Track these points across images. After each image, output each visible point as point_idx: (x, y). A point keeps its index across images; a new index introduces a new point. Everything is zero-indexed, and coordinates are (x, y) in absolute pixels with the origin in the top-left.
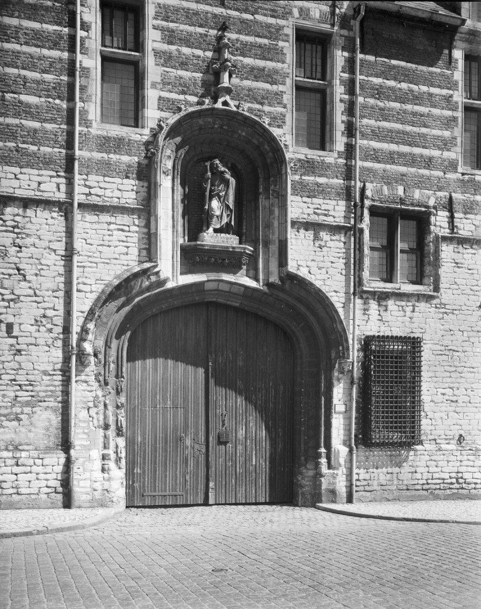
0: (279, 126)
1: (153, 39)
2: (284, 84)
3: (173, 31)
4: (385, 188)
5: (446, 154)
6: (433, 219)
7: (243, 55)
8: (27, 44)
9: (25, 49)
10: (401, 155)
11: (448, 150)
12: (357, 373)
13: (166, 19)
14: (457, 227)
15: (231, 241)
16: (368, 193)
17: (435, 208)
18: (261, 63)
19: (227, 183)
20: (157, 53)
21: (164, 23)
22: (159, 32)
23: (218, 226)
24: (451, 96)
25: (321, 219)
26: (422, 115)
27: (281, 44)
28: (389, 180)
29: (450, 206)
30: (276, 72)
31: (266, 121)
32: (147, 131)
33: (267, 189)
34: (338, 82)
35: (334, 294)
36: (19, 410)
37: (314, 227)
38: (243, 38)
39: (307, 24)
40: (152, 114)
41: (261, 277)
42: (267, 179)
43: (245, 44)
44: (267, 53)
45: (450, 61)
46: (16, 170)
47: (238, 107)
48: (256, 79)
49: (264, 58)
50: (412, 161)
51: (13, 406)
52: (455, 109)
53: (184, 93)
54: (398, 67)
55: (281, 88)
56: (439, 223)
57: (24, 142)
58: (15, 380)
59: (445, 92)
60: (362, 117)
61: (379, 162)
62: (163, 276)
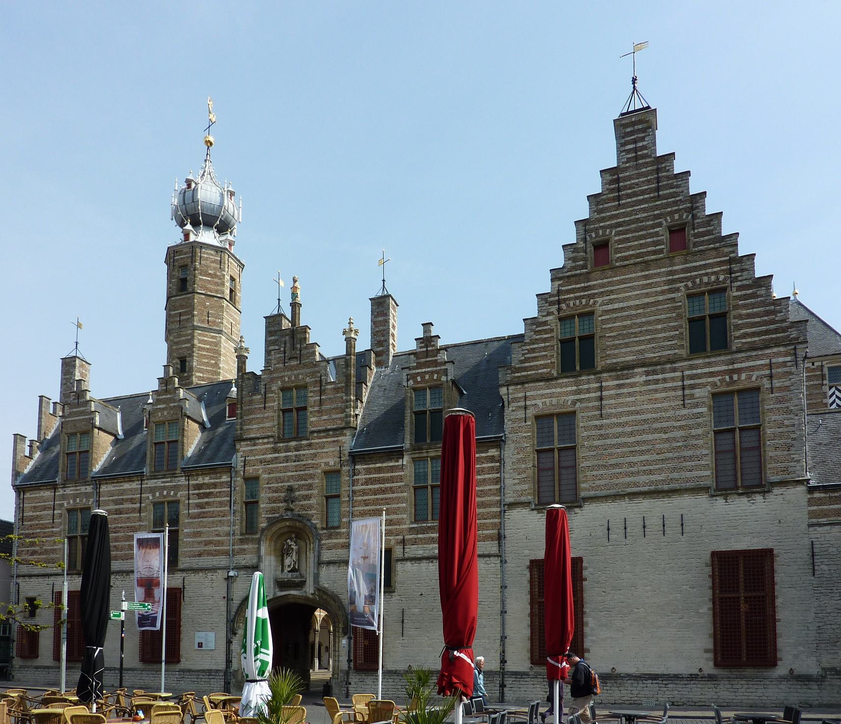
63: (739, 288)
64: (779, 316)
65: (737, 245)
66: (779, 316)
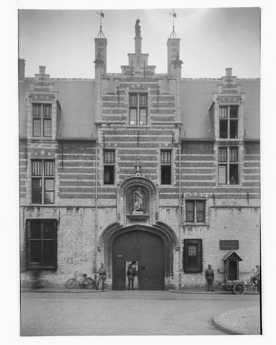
0: (155, 179)
1: (118, 160)
2: (157, 166)
3: (123, 156)
4: (190, 194)
5: (211, 181)
6: (207, 202)
7: (144, 160)
10: (195, 183)
11: (212, 180)
12: (182, 250)
13: (122, 154)
14: (216, 203)
15: (141, 213)
16: (185, 196)
17: (208, 198)
18: (149, 162)
19: (140, 197)
20: (119, 163)
21: (120, 155)
22: (119, 158)
23: (137, 209)
24: (213, 163)
25: (169, 205)
26: (202, 170)
27: (156, 155)
28: (192, 191)
29: (214, 197)
30: (154, 163)
31: (150, 179)
32: (116, 185)
33: (152, 198)
34: (174, 164)
35: (174, 227)
37: (168, 208)
38: (144, 155)
39: (164, 148)
40: (117, 180)
41: (151, 223)
42: (152, 194)
43: (144, 157)
44: (150, 158)
45: (213, 152)
46: (81, 199)
47: (141, 175)
48: (148, 166)
49: (151, 160)
50: (200, 184)
51: (81, 261)
52: (215, 166)
53: (127, 173)
54: (194, 156)
55: (156, 168)
56: (210, 203)
57: (83, 192)
58: (81, 254)
59: (211, 162)
60: (183, 173)
61: (188, 186)
62: (121, 225)
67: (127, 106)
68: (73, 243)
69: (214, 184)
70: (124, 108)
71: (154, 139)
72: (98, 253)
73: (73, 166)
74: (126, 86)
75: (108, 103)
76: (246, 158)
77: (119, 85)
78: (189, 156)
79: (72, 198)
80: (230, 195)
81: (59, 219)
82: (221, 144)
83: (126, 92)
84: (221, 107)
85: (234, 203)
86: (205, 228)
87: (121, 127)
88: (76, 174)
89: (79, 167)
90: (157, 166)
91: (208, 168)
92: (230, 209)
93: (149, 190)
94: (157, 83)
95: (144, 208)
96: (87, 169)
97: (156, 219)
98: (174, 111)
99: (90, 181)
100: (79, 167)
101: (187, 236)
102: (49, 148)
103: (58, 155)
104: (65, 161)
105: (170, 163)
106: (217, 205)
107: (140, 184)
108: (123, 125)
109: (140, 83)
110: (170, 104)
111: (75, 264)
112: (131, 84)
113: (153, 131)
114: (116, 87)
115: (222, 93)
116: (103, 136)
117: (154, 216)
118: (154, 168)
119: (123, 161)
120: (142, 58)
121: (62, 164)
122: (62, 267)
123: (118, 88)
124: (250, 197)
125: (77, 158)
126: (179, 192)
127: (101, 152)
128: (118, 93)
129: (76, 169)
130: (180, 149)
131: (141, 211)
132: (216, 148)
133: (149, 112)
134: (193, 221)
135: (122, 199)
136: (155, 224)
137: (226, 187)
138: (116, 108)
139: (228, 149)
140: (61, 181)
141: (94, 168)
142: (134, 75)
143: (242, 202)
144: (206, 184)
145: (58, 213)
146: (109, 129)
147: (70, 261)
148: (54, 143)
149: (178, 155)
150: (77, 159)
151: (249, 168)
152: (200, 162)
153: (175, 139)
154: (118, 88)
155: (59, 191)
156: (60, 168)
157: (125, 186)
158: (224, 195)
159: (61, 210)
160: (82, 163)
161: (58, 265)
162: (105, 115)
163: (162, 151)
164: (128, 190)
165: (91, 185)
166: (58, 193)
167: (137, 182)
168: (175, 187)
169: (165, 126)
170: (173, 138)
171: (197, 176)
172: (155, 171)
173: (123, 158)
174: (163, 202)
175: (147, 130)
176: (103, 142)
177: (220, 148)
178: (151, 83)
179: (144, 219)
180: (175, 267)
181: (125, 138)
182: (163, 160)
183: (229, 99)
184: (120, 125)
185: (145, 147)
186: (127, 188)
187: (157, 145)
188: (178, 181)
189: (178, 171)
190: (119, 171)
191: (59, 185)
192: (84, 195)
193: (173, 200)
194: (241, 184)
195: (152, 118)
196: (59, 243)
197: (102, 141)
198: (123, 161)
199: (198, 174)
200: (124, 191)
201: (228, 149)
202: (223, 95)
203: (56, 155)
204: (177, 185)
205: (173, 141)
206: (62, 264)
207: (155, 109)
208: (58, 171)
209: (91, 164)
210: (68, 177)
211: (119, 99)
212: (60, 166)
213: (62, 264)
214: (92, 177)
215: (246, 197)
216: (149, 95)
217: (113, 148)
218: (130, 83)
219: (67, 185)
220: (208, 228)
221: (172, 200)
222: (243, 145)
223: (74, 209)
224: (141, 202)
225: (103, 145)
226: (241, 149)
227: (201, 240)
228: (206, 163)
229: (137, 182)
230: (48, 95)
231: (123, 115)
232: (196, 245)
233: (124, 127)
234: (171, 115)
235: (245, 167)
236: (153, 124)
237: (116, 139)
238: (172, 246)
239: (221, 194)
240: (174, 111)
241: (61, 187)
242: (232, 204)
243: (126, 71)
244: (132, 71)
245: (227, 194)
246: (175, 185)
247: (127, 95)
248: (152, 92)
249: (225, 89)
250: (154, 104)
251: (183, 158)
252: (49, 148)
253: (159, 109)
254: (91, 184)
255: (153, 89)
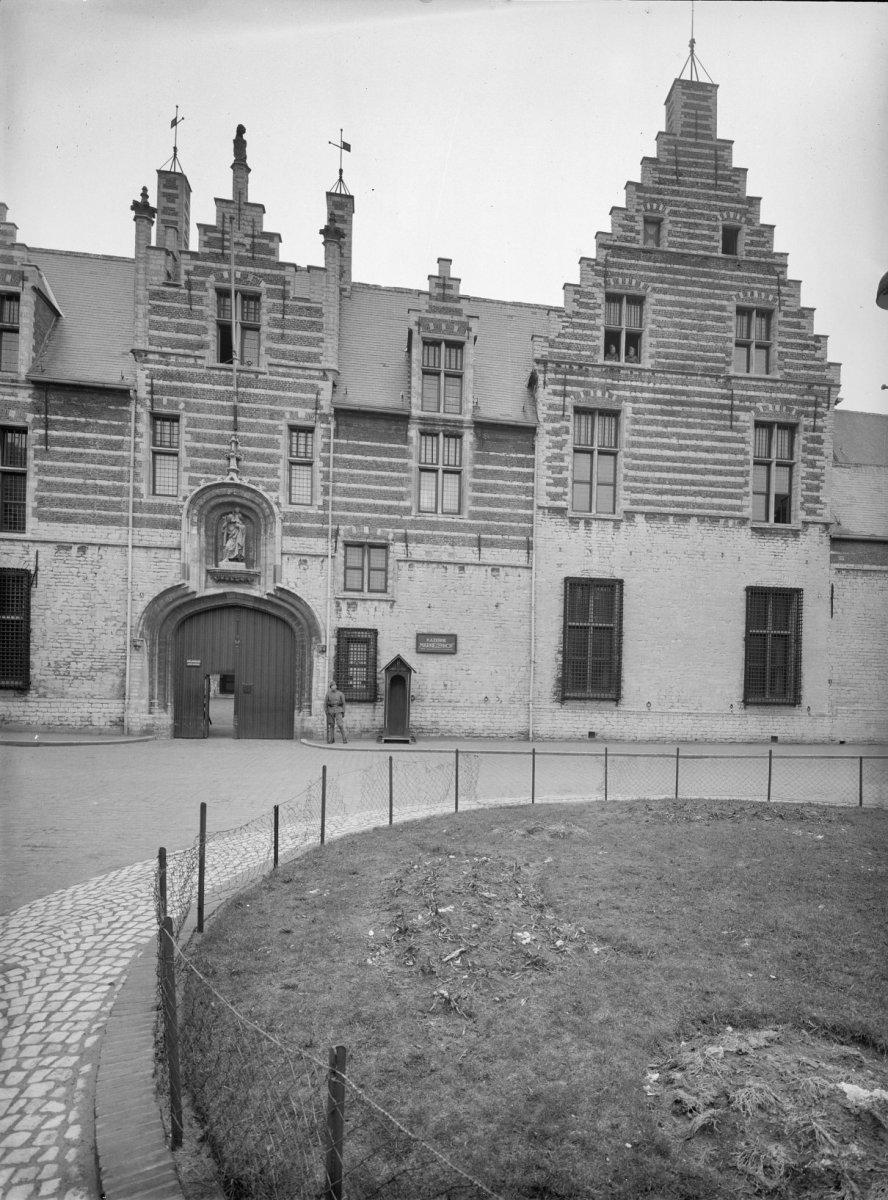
0: (274, 491)
4: (354, 528)
5: (402, 503)
6: (391, 548)
7: (249, 446)
8: (100, 448)
9: (100, 451)
10: (366, 505)
12: (331, 652)
15: (241, 566)
16: (341, 532)
23: (232, 557)
25: (305, 551)
27: (276, 436)
28: (357, 522)
29: (405, 539)
30: (273, 455)
31: (260, 489)
33: (266, 531)
36: (94, 674)
37: (303, 559)
43: (250, 439)
45: (406, 440)
46: (93, 526)
49: (264, 447)
53: (206, 473)
55: (277, 465)
56: (397, 549)
62: (190, 590)
63: (786, 314)
64: (818, 354)
65: (787, 266)
66: (818, 354)
67: (210, 319)
68: (70, 629)
69: (407, 511)
70: (203, 323)
71: (273, 400)
72: (136, 654)
73: (72, 447)
74: (207, 272)
75: (164, 307)
76: (478, 459)
77: (191, 268)
78: (353, 445)
79: (70, 522)
80: (441, 536)
81: (37, 569)
82: (421, 424)
83: (208, 285)
84: (427, 343)
85: (451, 554)
86: (385, 606)
87: (195, 366)
88: (81, 465)
89: (87, 451)
90: (278, 462)
91: (395, 474)
92: (441, 566)
93: (261, 515)
94: (282, 273)
95: (247, 556)
96: (110, 457)
97: (275, 582)
98: (322, 340)
99: (118, 484)
100: (87, 451)
101: (344, 623)
102: (12, 398)
103: (34, 419)
104: (53, 433)
105: (312, 458)
106: (415, 557)
107: (238, 500)
108: (200, 362)
109: (242, 268)
110: (314, 323)
111: (76, 678)
112: (220, 270)
113: (272, 381)
114: (183, 272)
115: (427, 311)
116: (149, 381)
117: (270, 573)
118: (272, 466)
119: (198, 445)
120: (249, 214)
121: (45, 440)
122: (43, 684)
123: (188, 273)
124: (483, 543)
125: (84, 427)
126: (328, 523)
127: (145, 418)
128: (189, 285)
129: (81, 454)
130: (332, 426)
131: (242, 561)
132: (413, 432)
133: (263, 337)
134: (362, 590)
135: (194, 531)
136: (273, 592)
137: (434, 519)
138: (183, 321)
139: (441, 435)
140: (41, 481)
141: (125, 454)
142: (228, 248)
143: (468, 554)
144: (389, 510)
145: (32, 556)
146: (165, 367)
147: (63, 670)
148: (26, 388)
149: (326, 440)
150: (83, 432)
151: (483, 481)
152: (378, 459)
153: (322, 403)
154: (188, 273)
155: (35, 504)
156: (41, 449)
157: (201, 502)
158: (428, 536)
159: (41, 548)
160: (95, 440)
161: (32, 679)
162: (155, 333)
163: (293, 428)
164: (210, 512)
165: (117, 495)
166: (34, 509)
167: (230, 496)
168: (321, 512)
169: (300, 372)
170: (317, 401)
171: (369, 490)
172: (274, 473)
173: (198, 438)
174: (292, 544)
175: (257, 377)
176: (149, 396)
177: (423, 433)
178: (268, 271)
179: (248, 579)
180: (317, 689)
181: (203, 390)
182: (294, 450)
183: (444, 327)
184: (192, 361)
185: (251, 417)
186: (208, 507)
187: (281, 415)
188: (326, 498)
189: (326, 477)
190: (189, 466)
191: (37, 490)
192: (100, 516)
193: (315, 539)
194: (466, 516)
195: (269, 351)
196: (37, 627)
197: (148, 393)
198: (198, 445)
199: (372, 487)
200: (200, 513)
201: (441, 435)
202: (431, 316)
203: (30, 417)
204: (325, 506)
205: (316, 409)
206: (44, 677)
207: (278, 331)
208: (35, 457)
209: (118, 446)
210: (60, 472)
211: (190, 300)
212: (41, 444)
213: (44, 677)
214: (119, 476)
215: (475, 543)
216: (264, 298)
217: (175, 412)
218: (218, 265)
219: (58, 490)
220: (392, 607)
221: (312, 541)
222: (472, 431)
223: (75, 548)
224: (241, 540)
225: (148, 403)
226: (469, 437)
227: (375, 632)
228: (390, 463)
229: (232, 495)
230: (11, 272)
231: (199, 338)
232: (366, 641)
233: (202, 367)
234: (315, 350)
235: (475, 477)
236: (270, 365)
237: (182, 392)
238: (311, 643)
239: (422, 532)
240: (322, 340)
241: (41, 494)
242: (445, 558)
243: (210, 238)
244: (223, 240)
245: (435, 533)
246: (320, 507)
247: (212, 293)
248: (271, 293)
249: (434, 303)
250: (275, 319)
251: (338, 448)
252: (12, 398)
253: (287, 332)
254: (119, 492)
255: (273, 286)
